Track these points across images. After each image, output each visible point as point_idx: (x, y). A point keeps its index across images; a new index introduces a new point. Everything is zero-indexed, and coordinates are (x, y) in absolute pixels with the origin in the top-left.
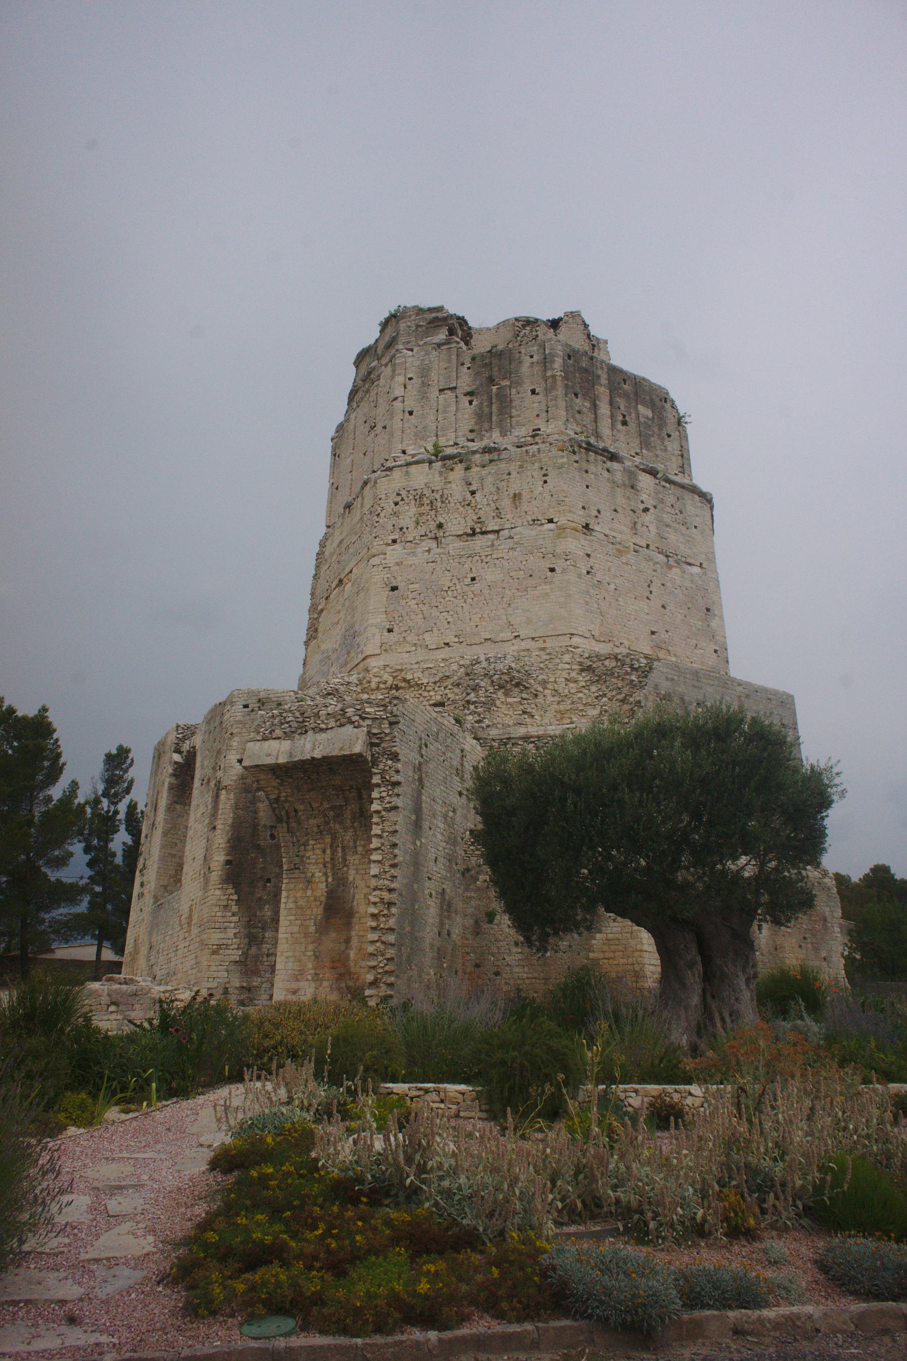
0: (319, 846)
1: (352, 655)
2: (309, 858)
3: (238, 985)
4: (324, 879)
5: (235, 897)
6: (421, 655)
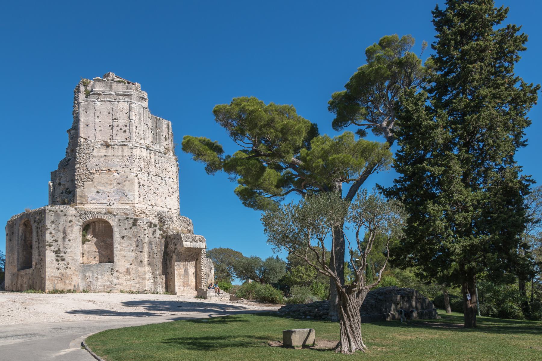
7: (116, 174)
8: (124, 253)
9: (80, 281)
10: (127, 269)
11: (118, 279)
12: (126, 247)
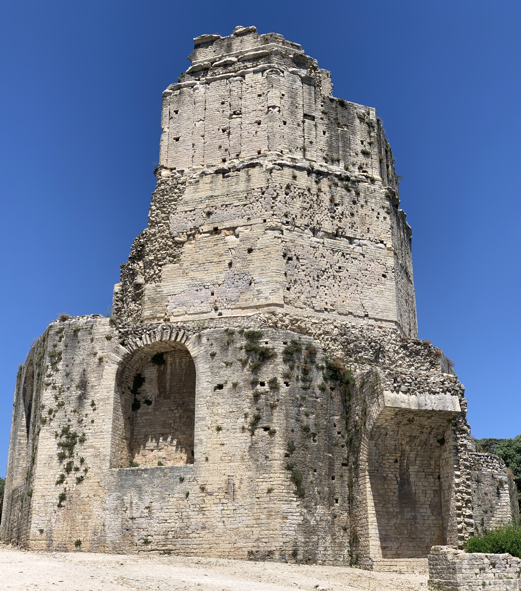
0: (393, 458)
1: (248, 295)
2: (384, 464)
3: (303, 540)
4: (395, 478)
6: (309, 311)
7: (231, 238)
11: (202, 510)
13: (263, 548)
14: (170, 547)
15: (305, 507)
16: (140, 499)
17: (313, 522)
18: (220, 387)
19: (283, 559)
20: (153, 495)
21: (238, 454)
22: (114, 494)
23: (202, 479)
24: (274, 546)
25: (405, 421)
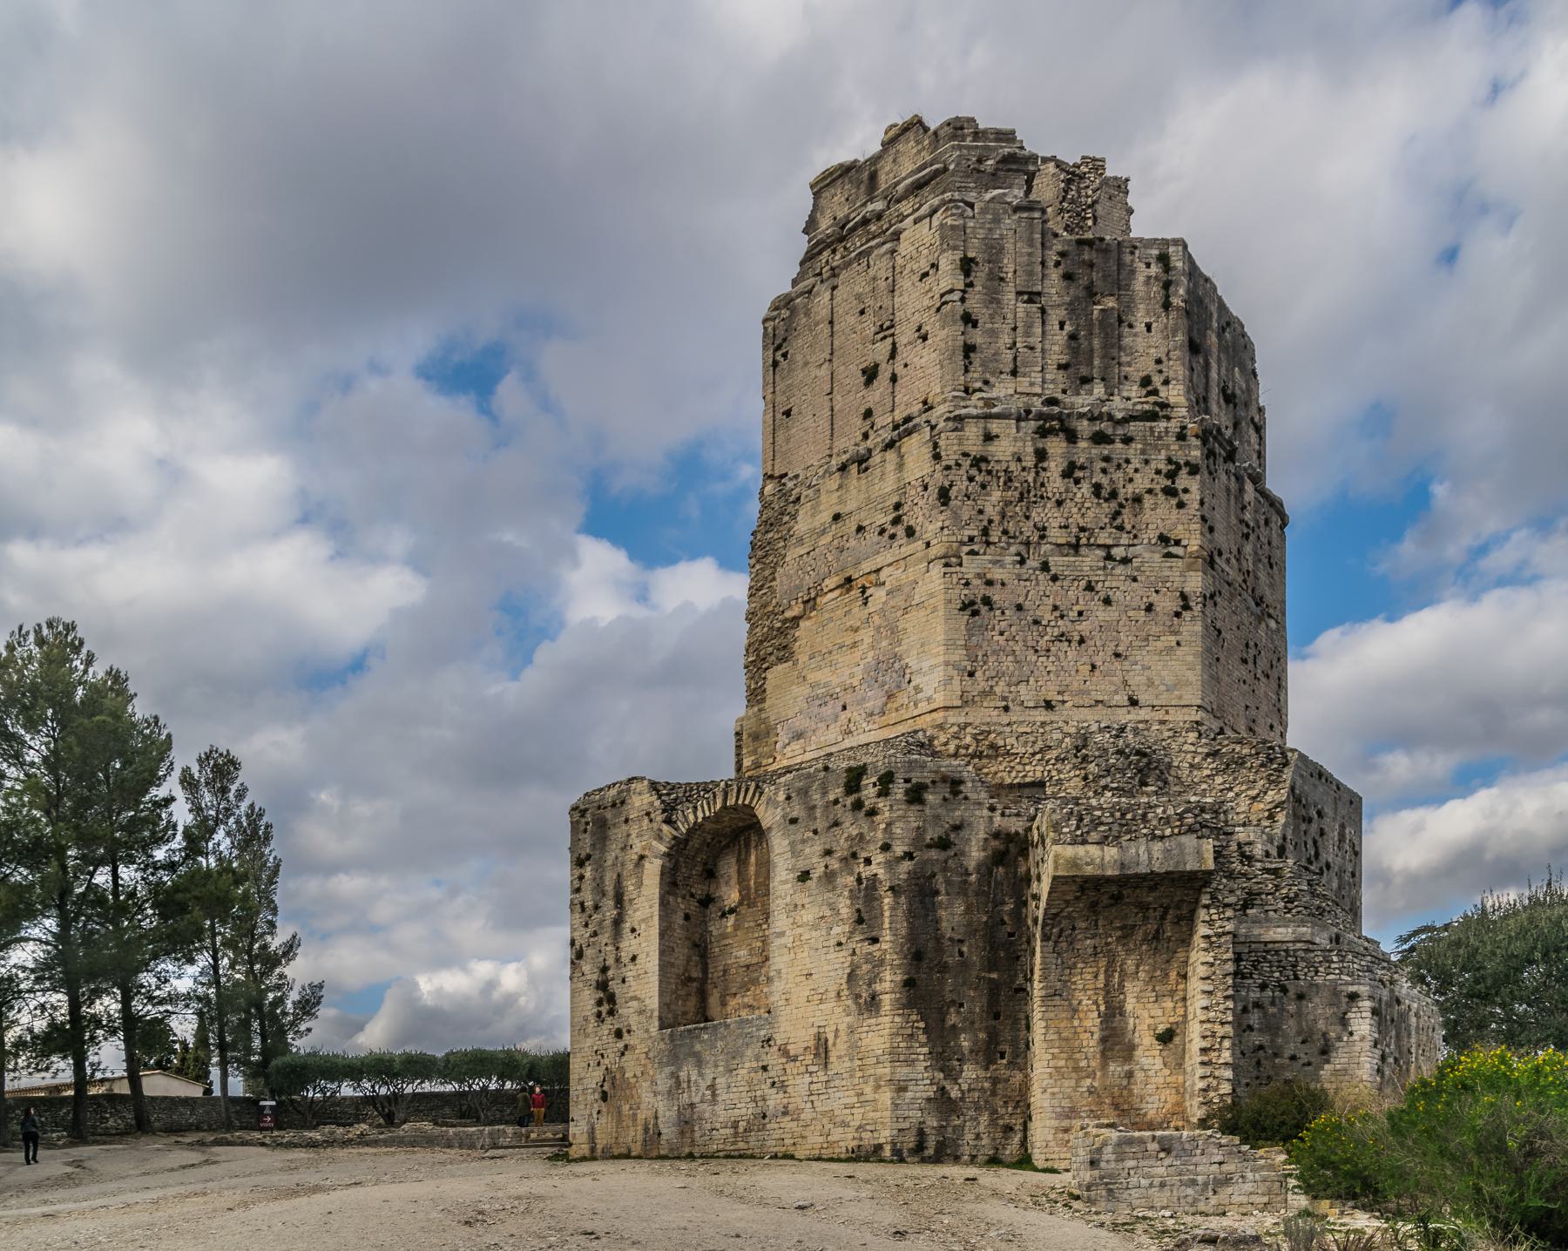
5: (922, 1025)
8: (805, 958)
9: (662, 1105)
10: (818, 1037)
12: (815, 927)
13: (868, 1139)
14: (741, 1145)
15: (942, 1070)
16: (701, 1074)
17: (954, 1093)
18: (804, 876)
19: (899, 1157)
20: (716, 1066)
21: (833, 989)
22: (668, 1070)
23: (783, 1036)
24: (885, 1135)
25: (1105, 900)
